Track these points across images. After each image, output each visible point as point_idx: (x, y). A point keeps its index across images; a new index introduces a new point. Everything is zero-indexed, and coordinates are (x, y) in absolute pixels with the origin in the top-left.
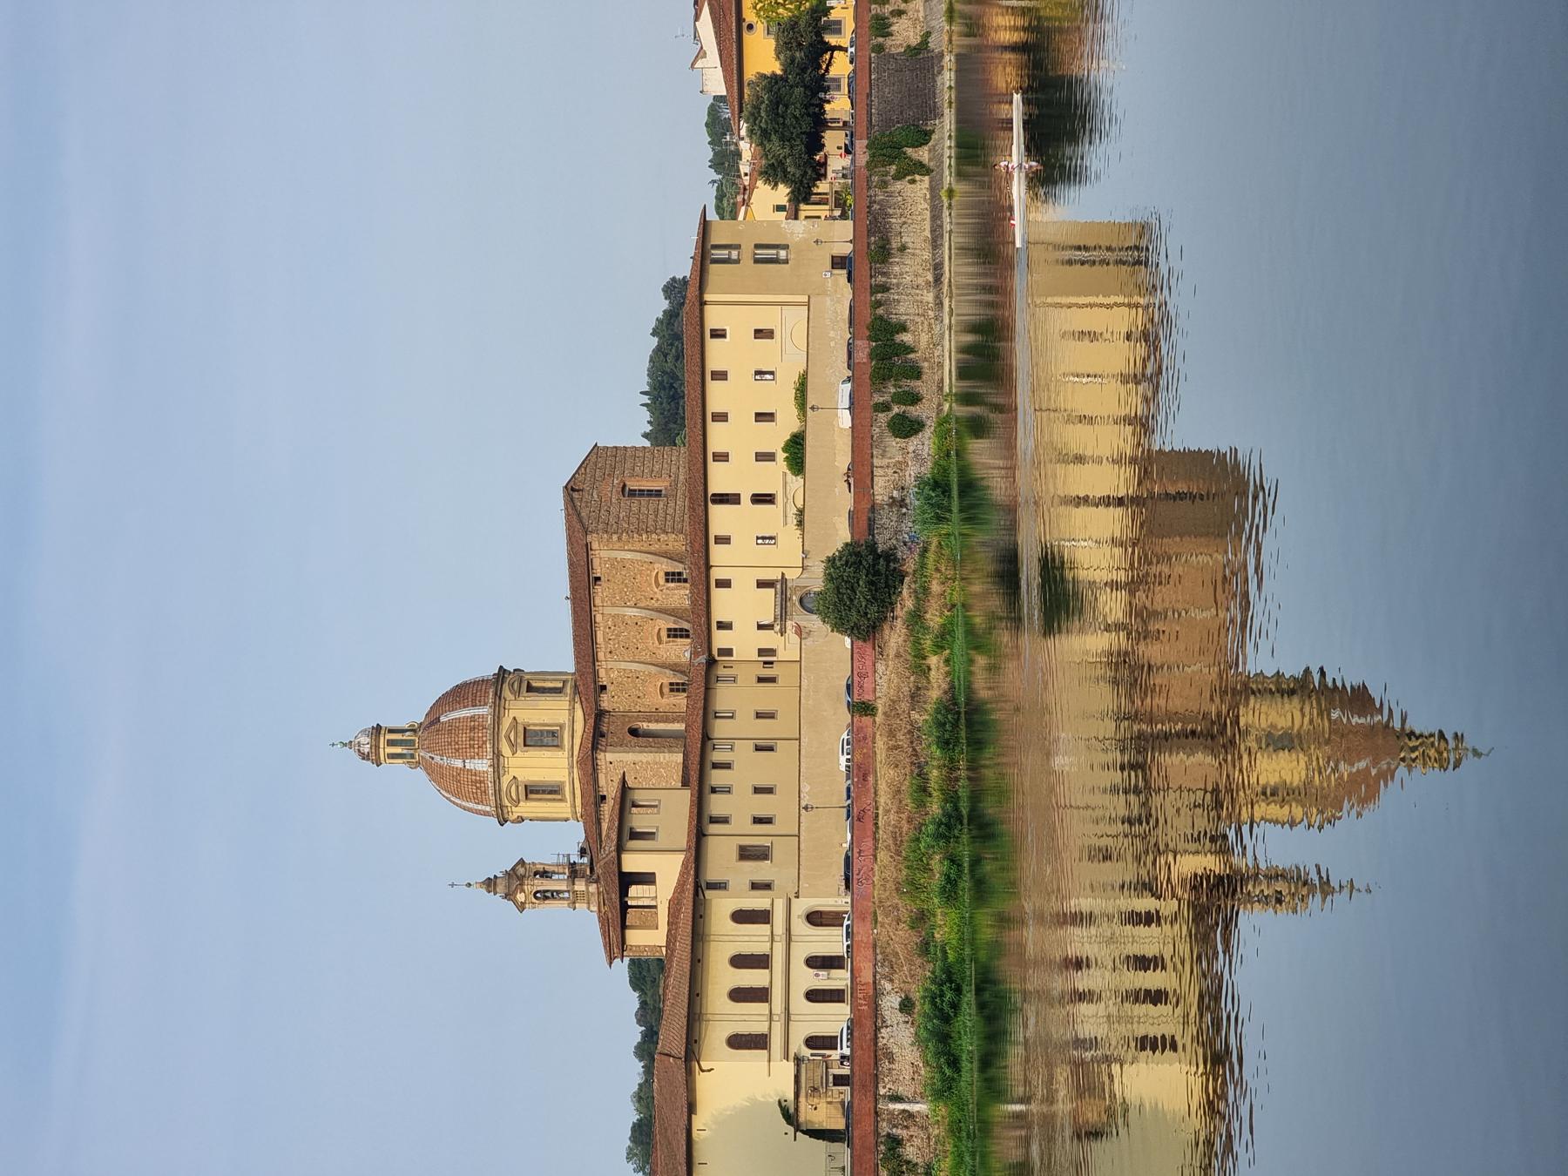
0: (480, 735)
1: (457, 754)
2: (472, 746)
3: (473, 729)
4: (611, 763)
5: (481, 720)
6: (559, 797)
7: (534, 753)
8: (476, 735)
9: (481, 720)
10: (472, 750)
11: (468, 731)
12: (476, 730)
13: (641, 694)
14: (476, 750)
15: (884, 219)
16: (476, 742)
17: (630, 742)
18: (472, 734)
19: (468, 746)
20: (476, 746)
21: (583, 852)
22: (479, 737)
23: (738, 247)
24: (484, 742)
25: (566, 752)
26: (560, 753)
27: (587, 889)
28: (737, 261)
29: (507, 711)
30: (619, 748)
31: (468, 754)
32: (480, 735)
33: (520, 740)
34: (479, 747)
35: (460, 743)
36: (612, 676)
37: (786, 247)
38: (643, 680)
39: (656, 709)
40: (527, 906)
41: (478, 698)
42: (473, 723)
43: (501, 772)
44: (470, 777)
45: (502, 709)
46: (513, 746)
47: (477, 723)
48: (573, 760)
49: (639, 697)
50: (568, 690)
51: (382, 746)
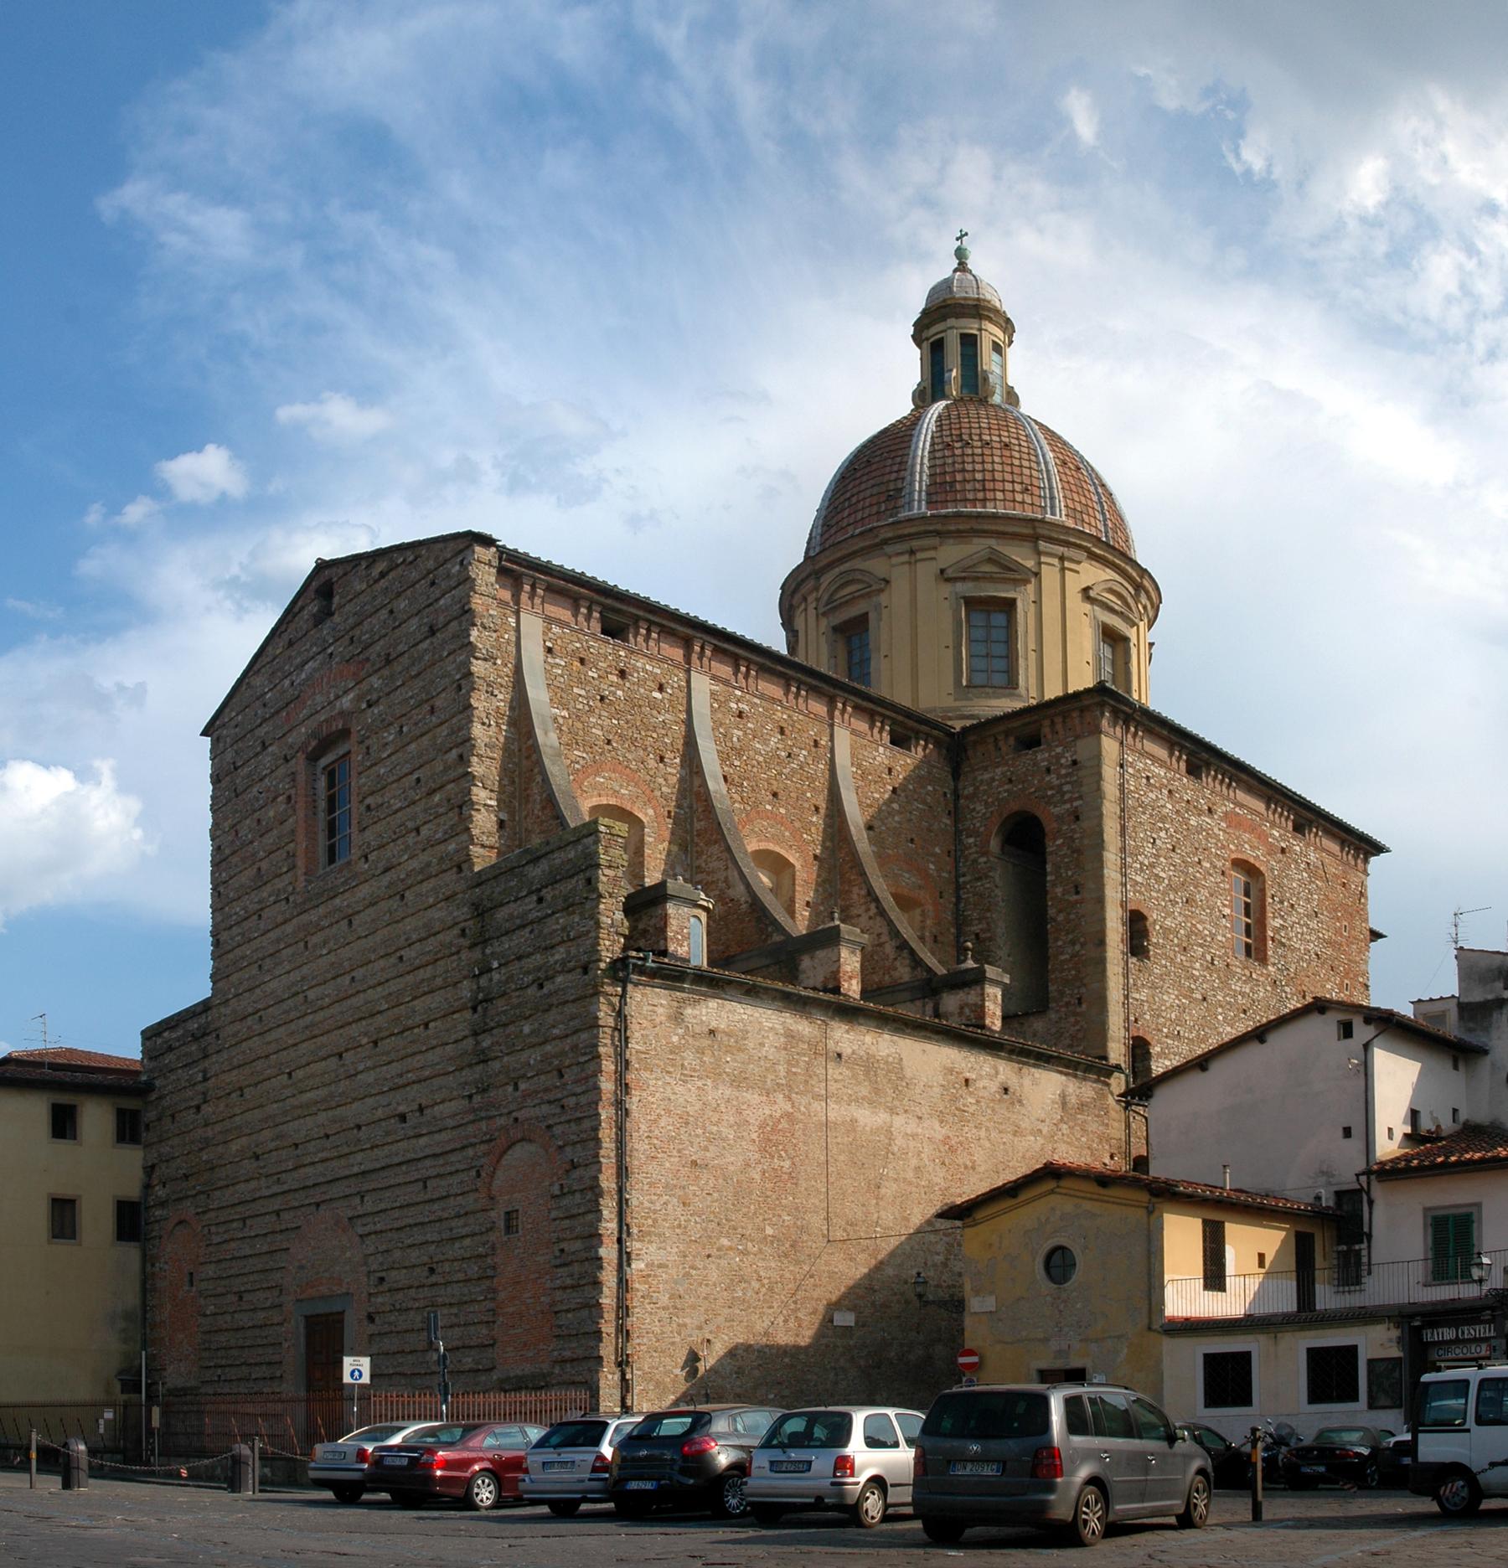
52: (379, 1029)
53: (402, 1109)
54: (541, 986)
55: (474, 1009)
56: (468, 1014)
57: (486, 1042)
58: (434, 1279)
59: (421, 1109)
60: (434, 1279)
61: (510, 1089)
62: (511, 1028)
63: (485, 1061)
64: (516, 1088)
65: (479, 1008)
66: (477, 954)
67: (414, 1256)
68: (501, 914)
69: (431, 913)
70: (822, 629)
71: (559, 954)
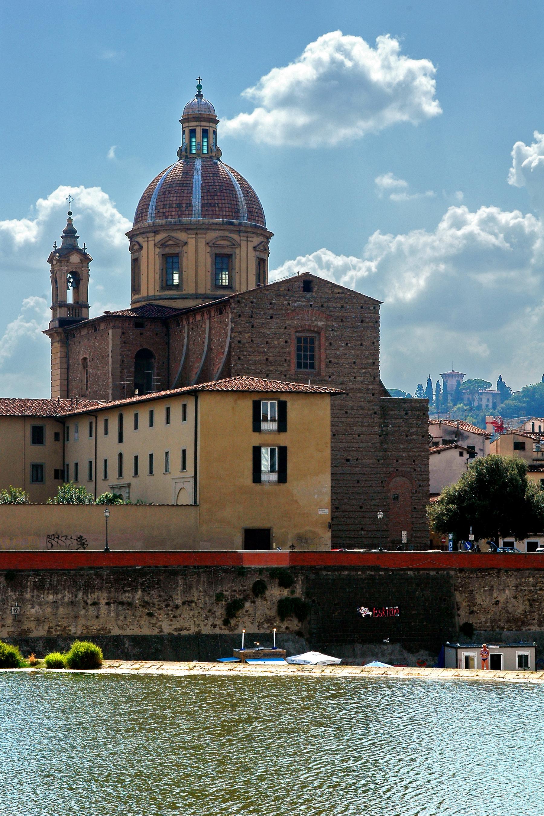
0: (174, 213)
2: (164, 206)
3: (179, 206)
7: (158, 261)
9: (187, 213)
10: (162, 207)
11: (178, 202)
12: (178, 209)
14: (161, 211)
15: (142, 584)
16: (167, 210)
18: (174, 206)
19: (165, 202)
23: (282, 427)
24: (167, 218)
25: (157, 293)
26: (157, 288)
28: (257, 428)
29: (194, 236)
31: (159, 204)
33: (167, 250)
34: (163, 213)
37: (283, 478)
41: (210, 209)
43: (144, 236)
44: (145, 206)
45: (195, 231)
46: (163, 245)
47: (184, 209)
48: (152, 300)
51: (192, 124)
52: (337, 431)
53: (348, 458)
54: (407, 436)
55: (380, 436)
56: (378, 437)
57: (385, 446)
58: (362, 510)
59: (357, 460)
60: (362, 510)
61: (395, 461)
62: (396, 445)
63: (386, 451)
64: (397, 461)
65: (383, 436)
66: (382, 421)
67: (354, 502)
68: (392, 413)
69: (361, 403)
70: (157, 253)
71: (414, 430)
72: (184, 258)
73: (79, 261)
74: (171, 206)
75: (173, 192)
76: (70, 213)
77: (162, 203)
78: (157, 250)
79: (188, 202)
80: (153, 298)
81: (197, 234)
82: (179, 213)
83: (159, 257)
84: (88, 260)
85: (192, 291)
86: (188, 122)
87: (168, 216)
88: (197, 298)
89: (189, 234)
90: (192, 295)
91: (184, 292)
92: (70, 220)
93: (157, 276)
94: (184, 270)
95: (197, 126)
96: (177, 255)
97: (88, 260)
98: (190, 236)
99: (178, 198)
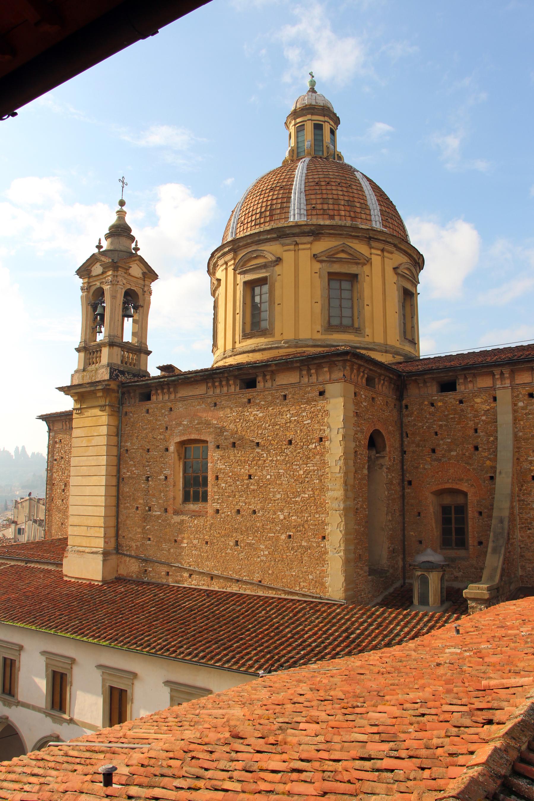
1: (312, 184)
2: (324, 201)
3: (350, 204)
4: (322, 393)
5: (363, 216)
6: (248, 331)
8: (342, 208)
9: (363, 216)
10: (319, 201)
11: (346, 198)
12: (348, 208)
13: (439, 454)
14: (319, 207)
17: (362, 431)
18: (342, 202)
19: (325, 196)
20: (325, 207)
21: (168, 369)
22: (339, 210)
24: (332, 217)
25: (319, 336)
26: (319, 328)
27: (103, 366)
30: (352, 407)
31: (313, 197)
32: (343, 213)
33: (337, 268)
35: (329, 187)
36: (478, 400)
38: (470, 458)
39: (410, 483)
40: (86, 280)
42: (358, 205)
43: (288, 241)
45: (381, 246)
47: (358, 210)
48: (308, 346)
49: (433, 451)
50: (408, 348)
72: (365, 285)
73: (140, 275)
74: (336, 202)
75: (333, 184)
76: (122, 203)
77: (319, 196)
78: (318, 266)
79: (362, 201)
80: (311, 343)
81: (383, 250)
82: (352, 214)
83: (320, 277)
84: (154, 276)
85: (379, 339)
86: (312, 114)
87: (334, 215)
88: (386, 352)
89: (371, 248)
90: (379, 345)
91: (367, 339)
92: (121, 214)
93: (318, 308)
94: (366, 303)
95: (324, 122)
96: (353, 278)
97: (154, 276)
98: (373, 251)
99: (346, 194)
